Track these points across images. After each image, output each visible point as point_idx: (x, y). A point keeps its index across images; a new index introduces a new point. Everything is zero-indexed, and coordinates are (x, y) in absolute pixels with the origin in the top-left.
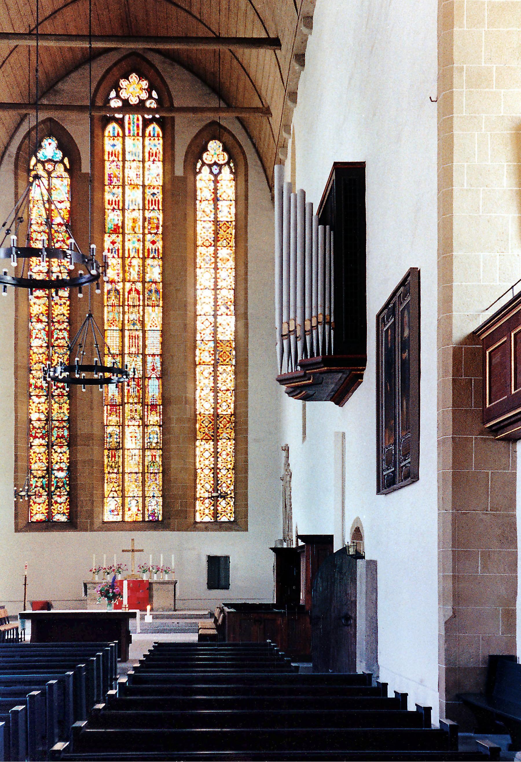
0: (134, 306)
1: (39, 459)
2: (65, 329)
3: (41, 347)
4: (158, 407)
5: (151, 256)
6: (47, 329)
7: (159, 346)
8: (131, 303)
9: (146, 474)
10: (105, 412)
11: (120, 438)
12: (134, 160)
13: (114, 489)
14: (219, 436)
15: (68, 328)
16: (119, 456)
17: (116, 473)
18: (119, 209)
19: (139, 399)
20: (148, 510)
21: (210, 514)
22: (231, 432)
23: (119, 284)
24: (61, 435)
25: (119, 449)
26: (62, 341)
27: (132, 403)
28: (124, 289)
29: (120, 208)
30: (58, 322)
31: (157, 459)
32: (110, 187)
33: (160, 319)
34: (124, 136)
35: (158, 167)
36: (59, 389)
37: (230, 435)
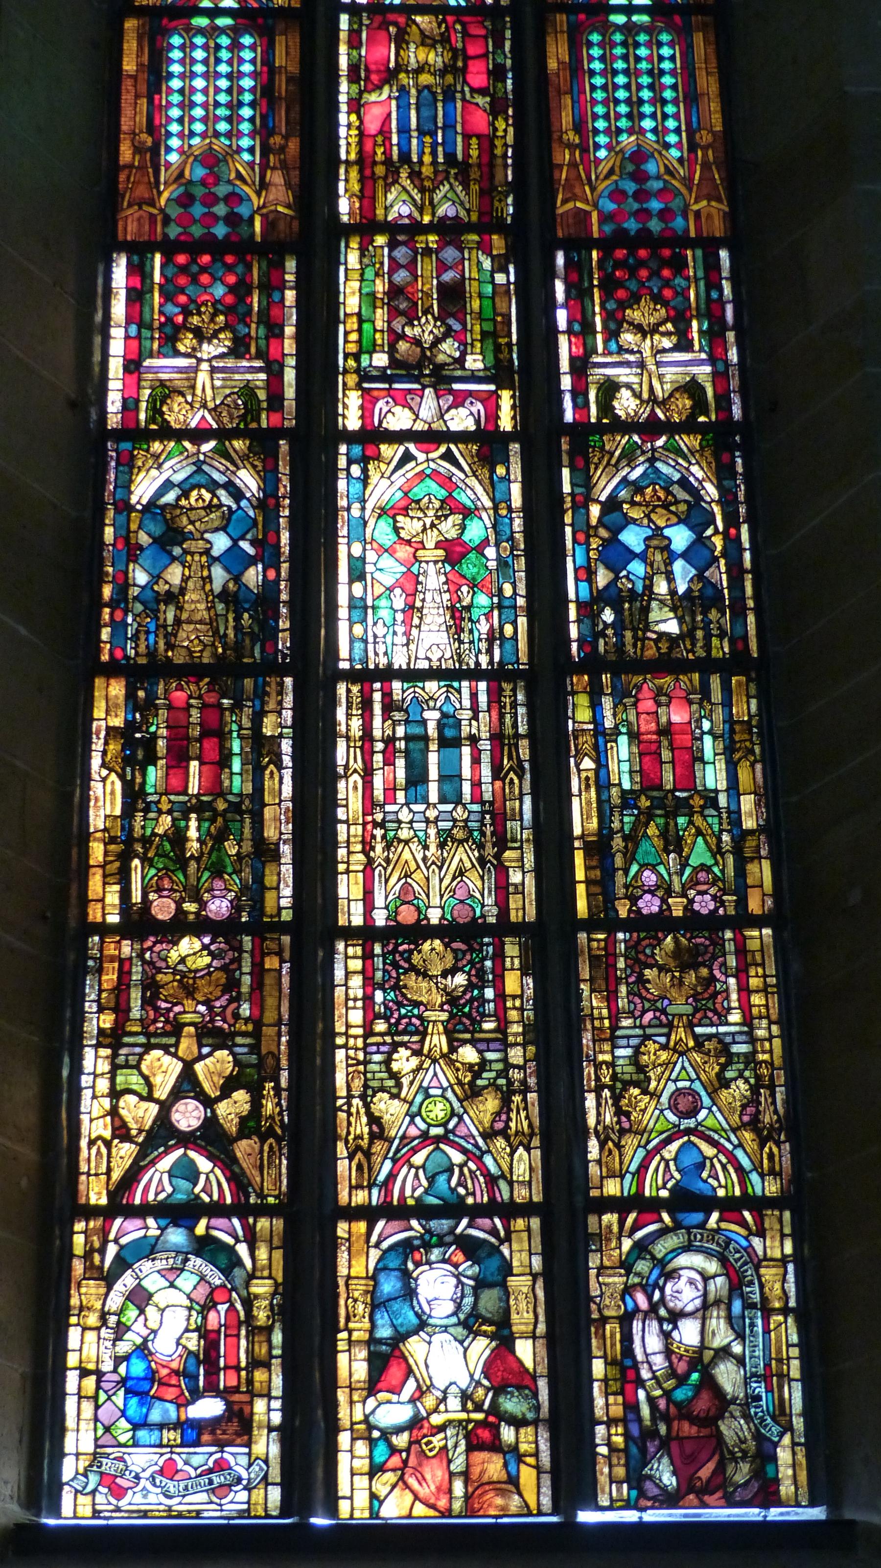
10: (119, 309)
19: (488, 193)
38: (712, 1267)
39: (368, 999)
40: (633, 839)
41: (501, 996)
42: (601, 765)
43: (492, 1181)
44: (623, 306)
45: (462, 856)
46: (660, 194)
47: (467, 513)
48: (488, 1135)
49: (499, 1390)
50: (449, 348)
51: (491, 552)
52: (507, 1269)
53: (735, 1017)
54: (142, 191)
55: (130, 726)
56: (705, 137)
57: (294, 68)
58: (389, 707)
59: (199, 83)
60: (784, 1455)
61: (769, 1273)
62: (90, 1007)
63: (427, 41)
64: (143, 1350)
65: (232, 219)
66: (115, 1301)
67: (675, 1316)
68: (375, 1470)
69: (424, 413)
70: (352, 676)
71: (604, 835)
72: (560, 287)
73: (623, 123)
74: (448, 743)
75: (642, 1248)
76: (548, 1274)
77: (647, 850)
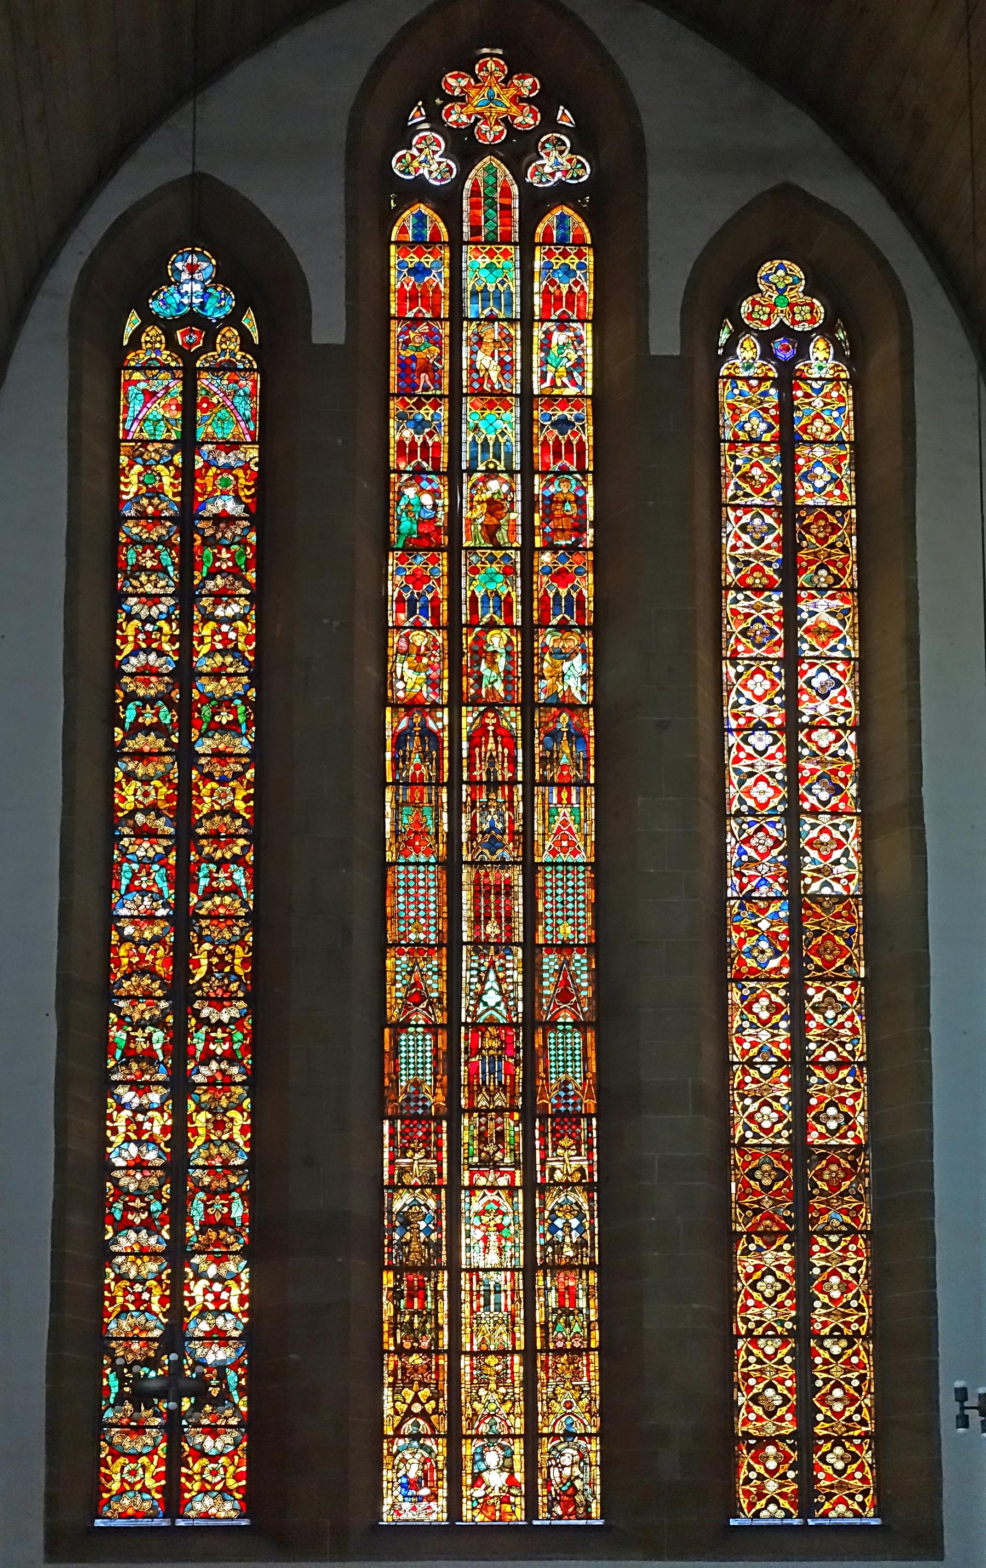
0: (493, 785)
1: (138, 1301)
2: (236, 859)
3: (151, 918)
4: (584, 1124)
5: (554, 622)
6: (172, 860)
7: (585, 915)
8: (480, 773)
9: (541, 1357)
10: (386, 1141)
11: (438, 1226)
12: (491, 319)
13: (416, 1408)
14: (815, 1221)
15: (250, 857)
16: (437, 1294)
17: (427, 1352)
18: (436, 471)
19: (513, 1097)
20: (548, 1482)
21: (784, 1496)
22: (857, 1209)
23: (439, 714)
24: (218, 1218)
25: (439, 1268)
26: (228, 900)
27: (483, 1112)
28: (455, 726)
29: (443, 466)
30: (214, 836)
31: (582, 1303)
32: (403, 402)
33: (590, 828)
34: (456, 245)
35: (580, 339)
36: (214, 1065)
37: (856, 1220)
38: (575, 1453)
39: (472, 1374)
40: (555, 1323)
41: (513, 1373)
42: (546, 1300)
43: (509, 1428)
44: (559, 1139)
45: (502, 1328)
46: (573, 1097)
47: (504, 1214)
48: (508, 1414)
49: (510, 1487)
50: (499, 1155)
51: (512, 1228)
52: (513, 1453)
53: (585, 1379)
54: (393, 1097)
55: (395, 1287)
56: (589, 1075)
57: (445, 1048)
58: (478, 1280)
59: (412, 1054)
60: (593, 1505)
61: (592, 1455)
62: (386, 1375)
63: (492, 1038)
64: (405, 1476)
65: (424, 1107)
66: (397, 1461)
67: (563, 1467)
68: (473, 1509)
69: (491, 1179)
70: (466, 1270)
71: (547, 1322)
72: (537, 1132)
73: (561, 1069)
74: (496, 1292)
75: (554, 1448)
76: (525, 1455)
77: (560, 1326)
